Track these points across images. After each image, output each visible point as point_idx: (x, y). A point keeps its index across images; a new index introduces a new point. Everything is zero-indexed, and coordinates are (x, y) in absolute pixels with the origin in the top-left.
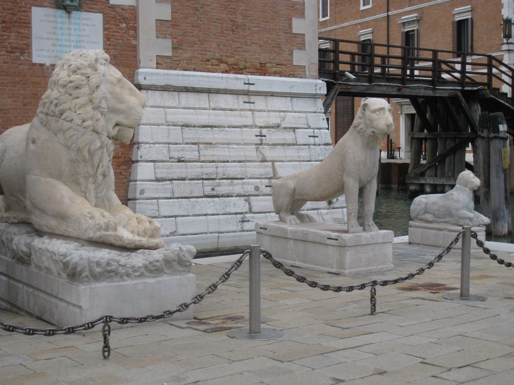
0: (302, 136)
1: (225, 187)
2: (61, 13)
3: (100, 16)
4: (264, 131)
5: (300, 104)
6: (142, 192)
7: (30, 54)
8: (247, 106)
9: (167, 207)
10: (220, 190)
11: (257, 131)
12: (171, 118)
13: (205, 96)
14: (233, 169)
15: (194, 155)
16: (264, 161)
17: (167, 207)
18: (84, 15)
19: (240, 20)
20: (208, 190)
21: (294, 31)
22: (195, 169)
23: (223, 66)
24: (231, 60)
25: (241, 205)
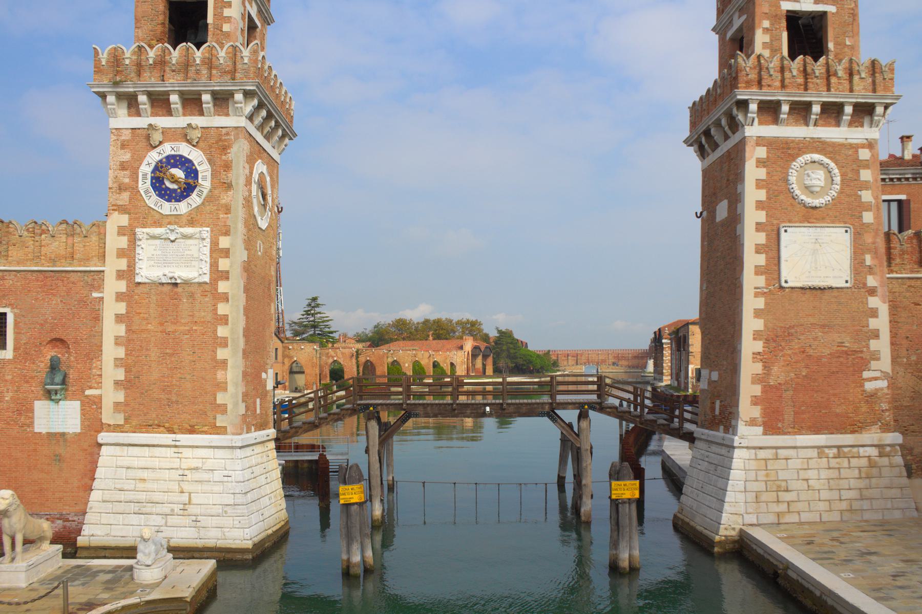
0: (217, 476)
1: (149, 508)
2: (51, 403)
3: (79, 402)
4: (186, 472)
5: (220, 453)
6: (91, 508)
7: (33, 427)
8: (176, 455)
9: (105, 519)
10: (144, 510)
11: (181, 472)
12: (119, 463)
13: (146, 448)
14: (157, 497)
15: (132, 487)
16: (182, 492)
17: (105, 519)
18: (68, 402)
19: (174, 399)
20: (136, 509)
21: (219, 401)
22: (131, 496)
23: (162, 429)
24: (167, 425)
25: (159, 520)
